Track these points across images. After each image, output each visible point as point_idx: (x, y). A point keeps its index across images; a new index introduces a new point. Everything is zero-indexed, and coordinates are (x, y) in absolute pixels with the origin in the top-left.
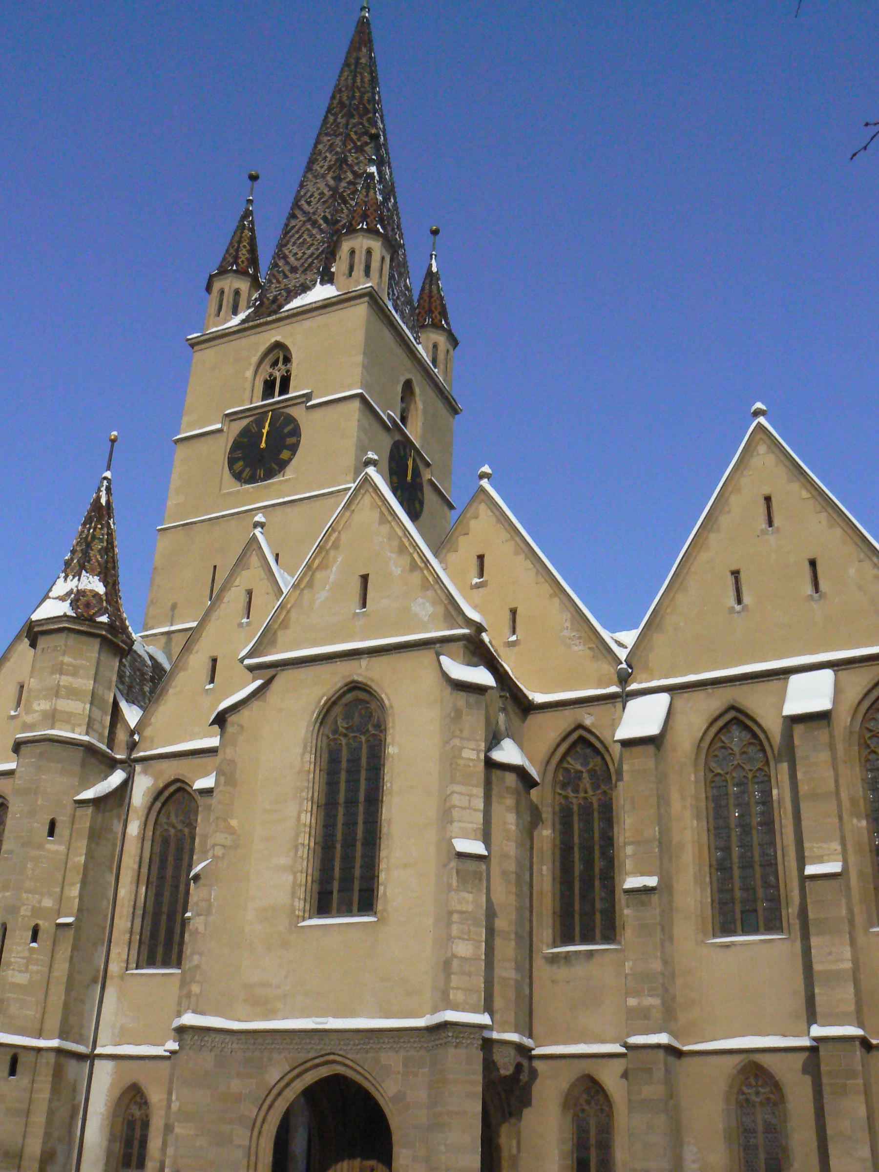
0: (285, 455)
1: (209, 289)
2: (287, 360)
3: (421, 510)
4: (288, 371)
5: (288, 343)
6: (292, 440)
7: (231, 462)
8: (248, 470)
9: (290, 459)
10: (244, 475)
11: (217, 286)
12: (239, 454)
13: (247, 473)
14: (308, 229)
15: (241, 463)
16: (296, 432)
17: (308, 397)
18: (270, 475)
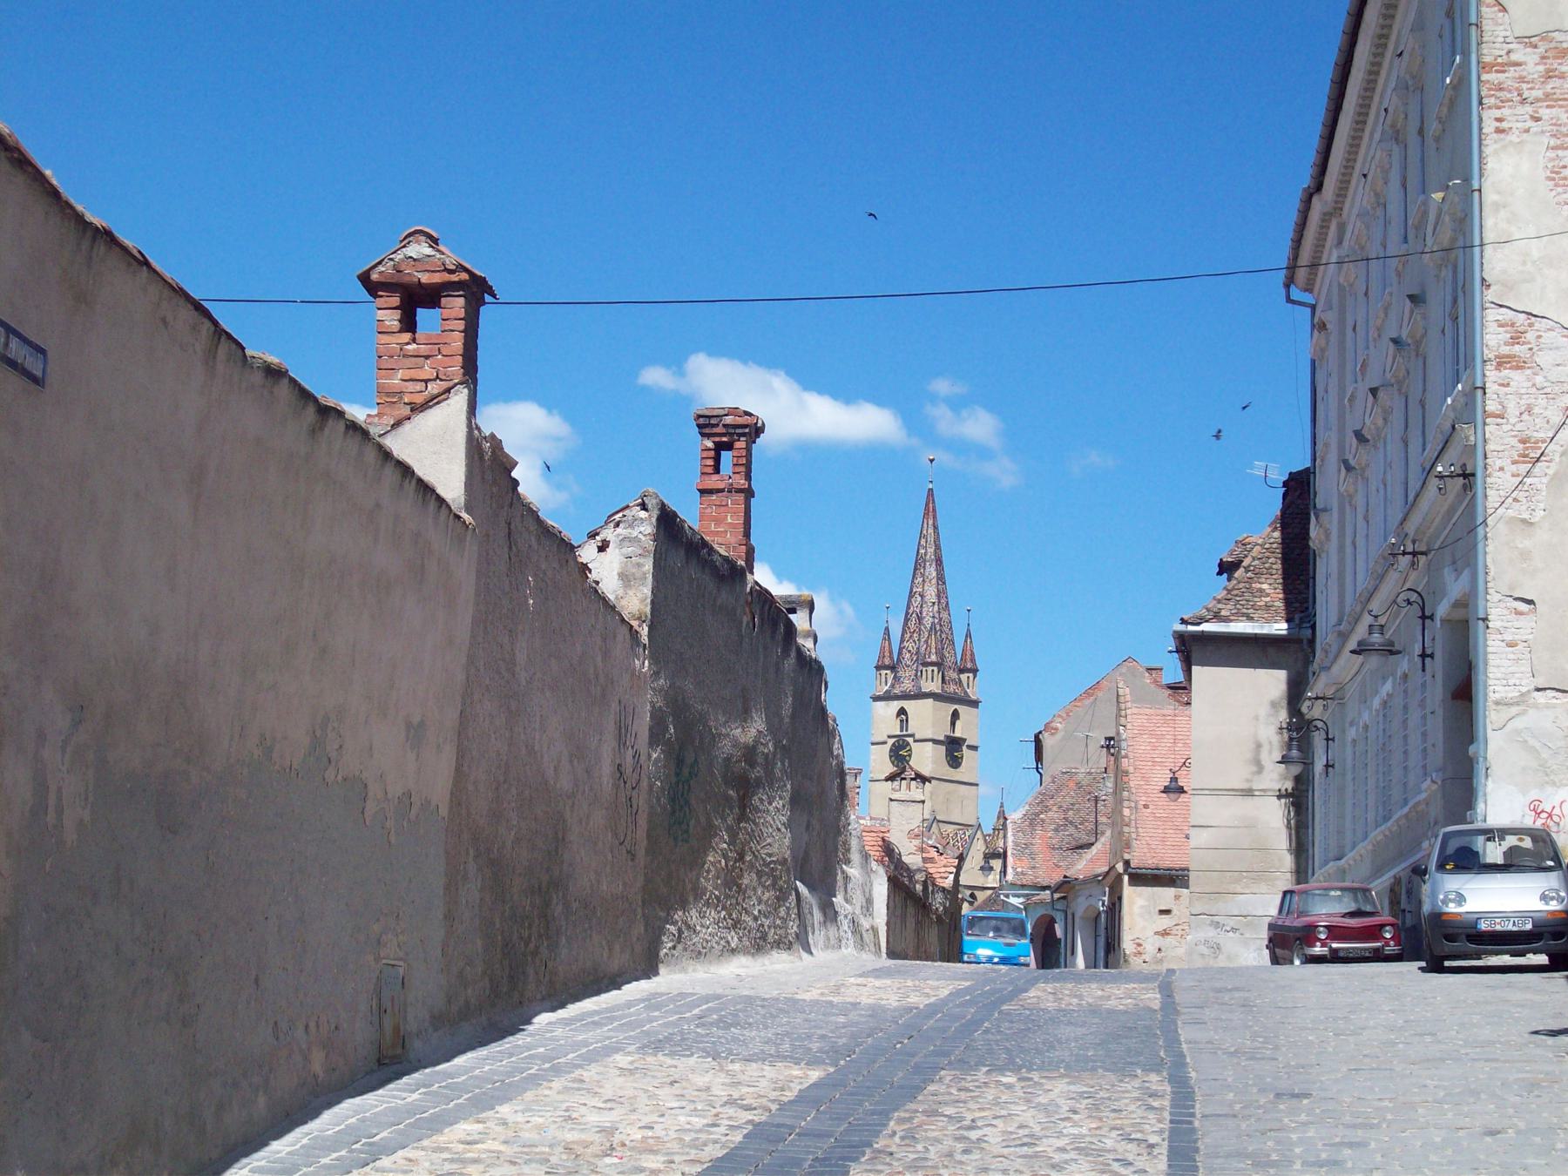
2: (906, 714)
7: (891, 757)
17: (912, 736)
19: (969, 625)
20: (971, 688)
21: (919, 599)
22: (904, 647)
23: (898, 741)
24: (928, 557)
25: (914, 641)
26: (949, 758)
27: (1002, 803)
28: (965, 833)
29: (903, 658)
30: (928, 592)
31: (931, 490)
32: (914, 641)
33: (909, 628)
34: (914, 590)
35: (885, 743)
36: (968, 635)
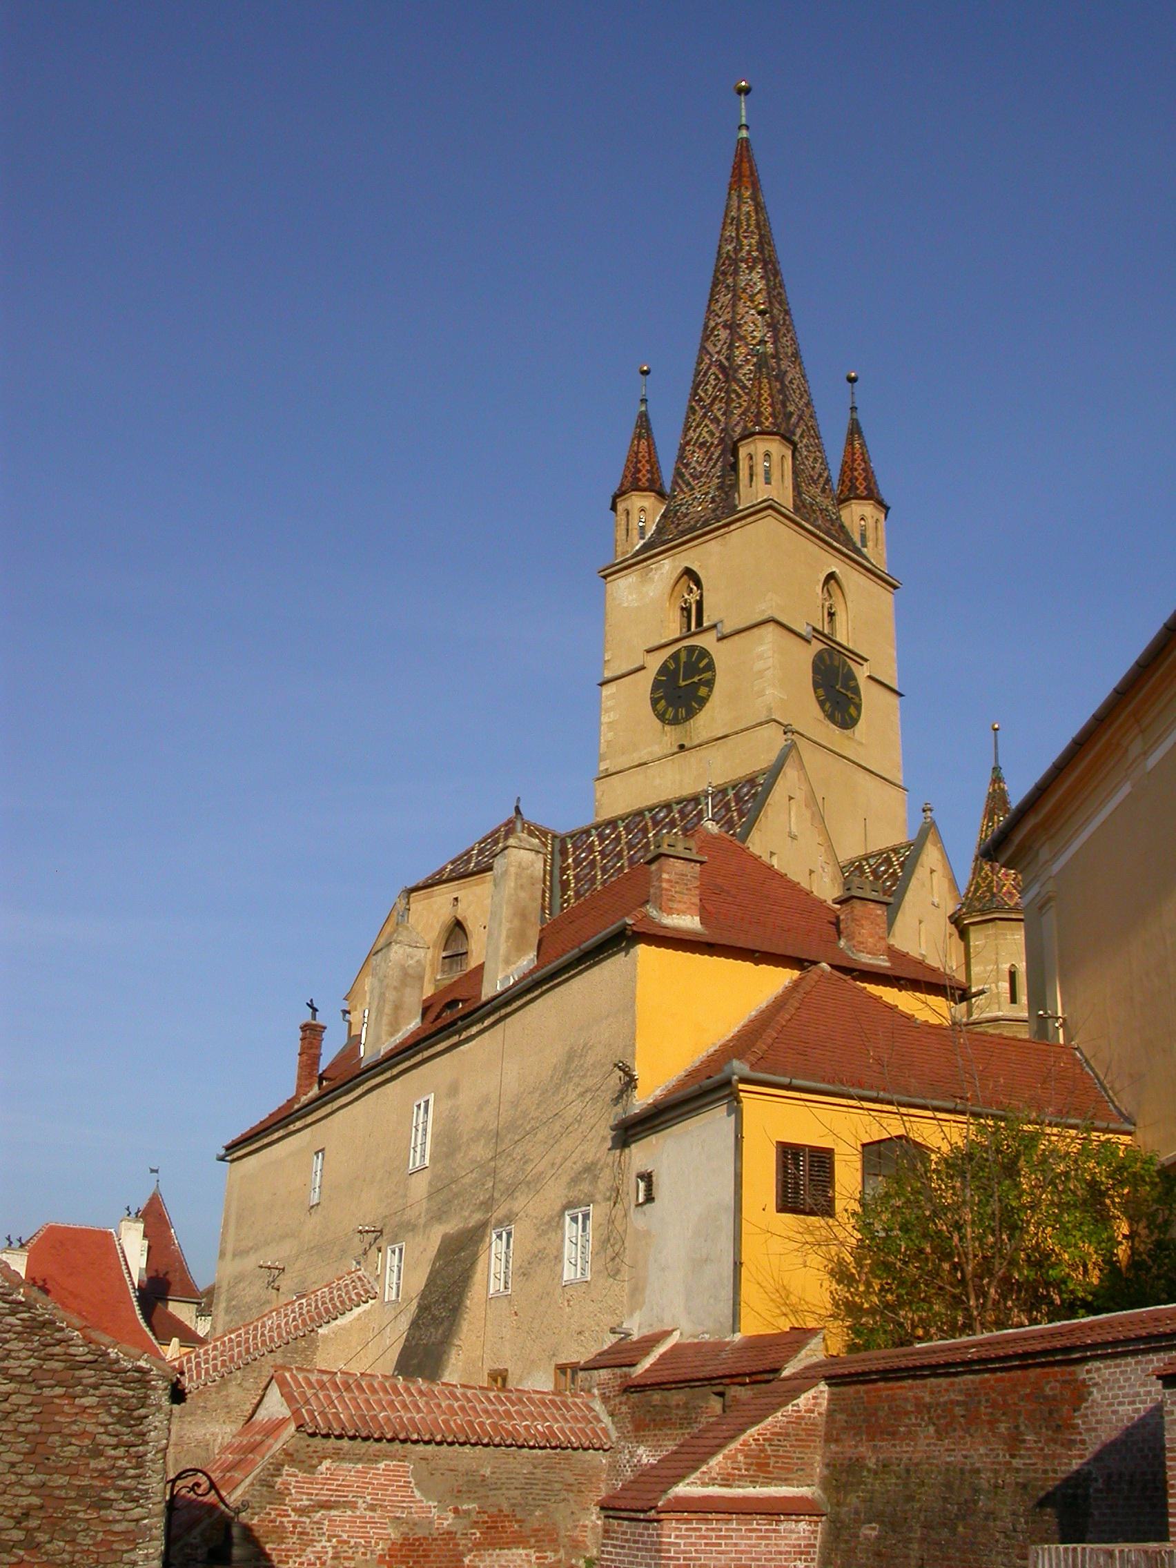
0: (703, 691)
1: (614, 508)
3: (859, 715)
4: (701, 596)
5: (695, 568)
6: (707, 675)
7: (655, 702)
8: (670, 709)
9: (709, 696)
10: (667, 717)
11: (620, 507)
12: (660, 694)
13: (670, 714)
14: (706, 426)
15: (663, 702)
16: (711, 667)
18: (691, 714)
19: (854, 409)
20: (870, 544)
21: (724, 334)
22: (688, 443)
23: (675, 657)
24: (744, 254)
25: (716, 420)
26: (821, 691)
27: (996, 769)
28: (888, 861)
29: (687, 466)
30: (748, 318)
31: (744, 145)
32: (716, 420)
33: (701, 400)
34: (712, 324)
35: (642, 668)
36: (855, 430)
